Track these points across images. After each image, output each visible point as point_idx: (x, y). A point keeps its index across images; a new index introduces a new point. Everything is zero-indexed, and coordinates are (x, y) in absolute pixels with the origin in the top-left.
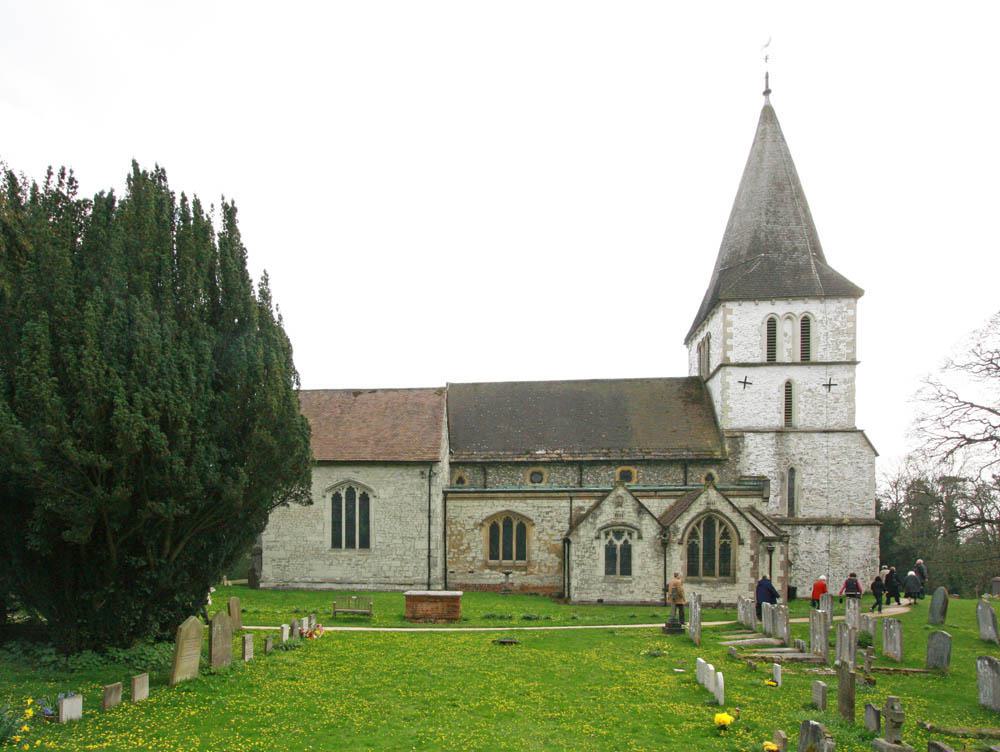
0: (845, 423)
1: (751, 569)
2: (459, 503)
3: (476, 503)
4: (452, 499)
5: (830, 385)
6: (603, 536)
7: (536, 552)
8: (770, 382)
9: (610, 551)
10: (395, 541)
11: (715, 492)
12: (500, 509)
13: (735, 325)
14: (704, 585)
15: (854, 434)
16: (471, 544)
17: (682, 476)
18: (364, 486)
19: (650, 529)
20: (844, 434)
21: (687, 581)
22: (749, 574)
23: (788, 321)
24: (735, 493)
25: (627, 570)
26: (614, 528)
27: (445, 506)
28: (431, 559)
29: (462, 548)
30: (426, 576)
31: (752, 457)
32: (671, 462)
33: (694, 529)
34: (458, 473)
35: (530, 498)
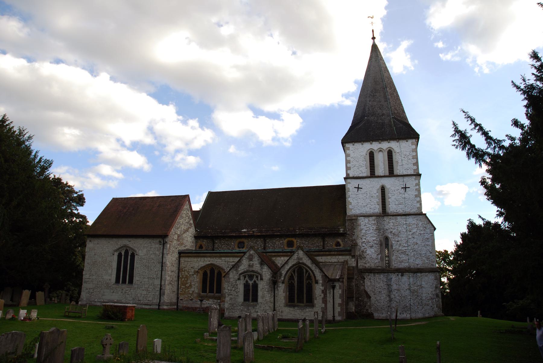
0: (418, 212)
1: (322, 298)
2: (187, 259)
3: (195, 259)
4: (183, 257)
5: (406, 188)
6: (242, 278)
8: (372, 186)
9: (246, 286)
10: (144, 280)
11: (302, 252)
13: (352, 155)
14: (296, 308)
15: (421, 216)
17: (322, 244)
19: (266, 273)
20: (414, 216)
21: (287, 305)
22: (321, 302)
23: (381, 153)
24: (336, 253)
25: (255, 299)
26: (248, 273)
27: (179, 261)
28: (162, 290)
29: (187, 285)
30: (158, 301)
31: (363, 231)
32: (315, 235)
33: (292, 274)
34: (200, 242)
35: (224, 256)
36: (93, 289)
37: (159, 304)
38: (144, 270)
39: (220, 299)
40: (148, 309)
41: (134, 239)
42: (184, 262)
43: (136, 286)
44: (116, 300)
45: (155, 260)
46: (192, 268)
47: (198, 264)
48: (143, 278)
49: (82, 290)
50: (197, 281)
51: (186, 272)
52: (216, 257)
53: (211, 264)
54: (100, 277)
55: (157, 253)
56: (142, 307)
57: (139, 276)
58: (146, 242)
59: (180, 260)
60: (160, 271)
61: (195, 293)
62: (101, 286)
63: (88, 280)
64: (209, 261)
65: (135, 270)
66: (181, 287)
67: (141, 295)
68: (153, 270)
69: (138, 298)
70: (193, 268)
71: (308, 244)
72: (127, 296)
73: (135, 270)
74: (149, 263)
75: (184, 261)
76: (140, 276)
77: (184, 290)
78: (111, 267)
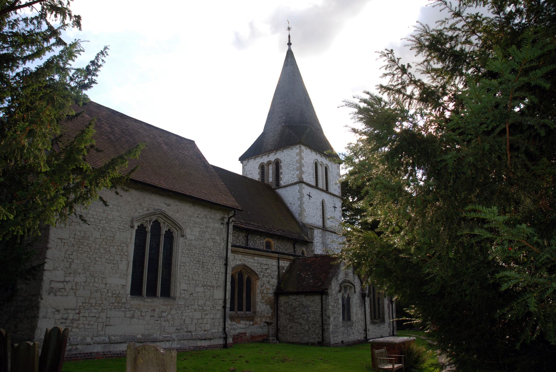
7: (259, 303)
10: (198, 289)
12: (238, 263)
14: (376, 325)
17: (292, 250)
18: (174, 223)
30: (221, 329)
36: (77, 311)
38: (196, 270)
39: (252, 320)
40: (207, 348)
41: (177, 203)
43: (181, 302)
44: (139, 336)
48: (194, 286)
49: (41, 315)
52: (248, 254)
53: (245, 265)
54: (96, 280)
55: (217, 238)
56: (195, 345)
57: (187, 282)
58: (199, 214)
60: (222, 273)
62: (100, 302)
63: (61, 285)
65: (180, 269)
67: (192, 321)
68: (211, 270)
71: (283, 249)
72: (163, 324)
73: (180, 269)
74: (204, 257)
78: (126, 255)
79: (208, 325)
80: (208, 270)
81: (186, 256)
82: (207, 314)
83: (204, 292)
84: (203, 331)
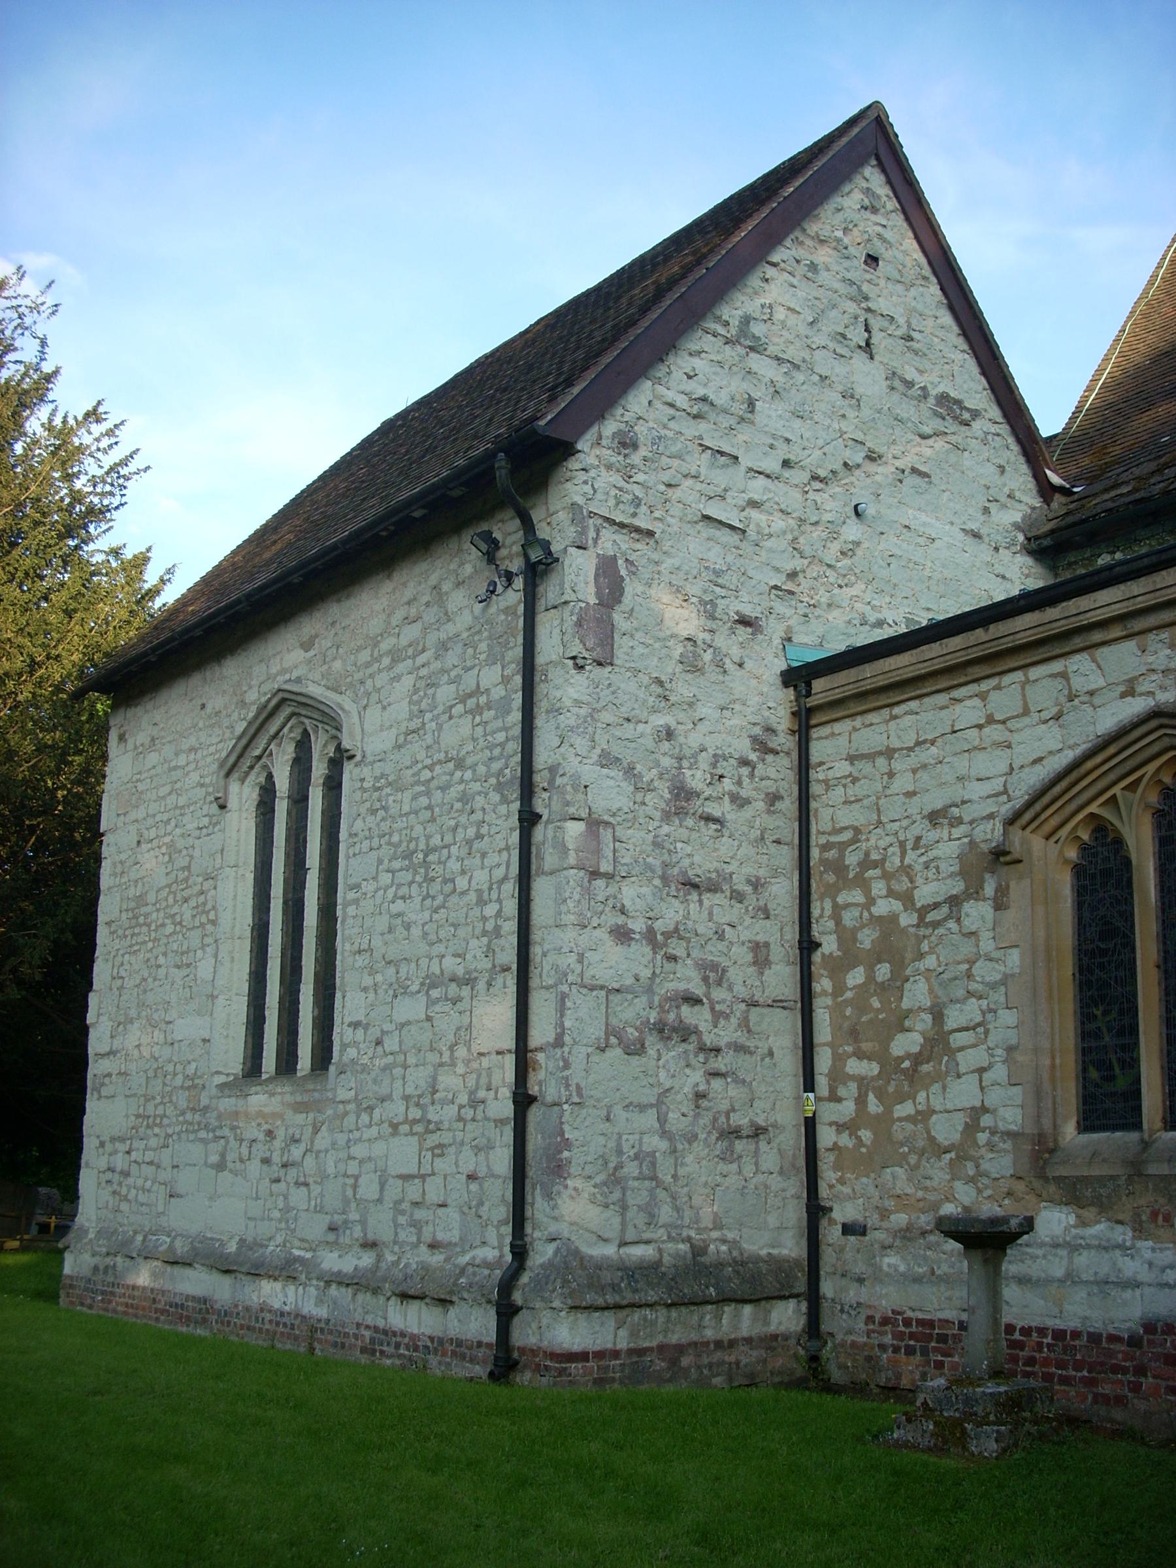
16: (954, 1017)
28: (534, 1114)
29: (906, 1044)
37: (507, 1284)
42: (843, 768)
45: (473, 767)
46: (934, 818)
47: (996, 763)
50: (1005, 980)
51: (878, 888)
56: (381, 1323)
57: (368, 981)
59: (815, 757)
61: (993, 1132)
64: (1130, 692)
66: (845, 1078)
69: (363, 1222)
70: (959, 821)
75: (851, 759)
76: (372, 972)
77: (874, 1105)
79: (452, 1215)
80: (449, 886)
81: (366, 844)
82: (439, 1150)
83: (429, 1019)
84: (423, 1248)
